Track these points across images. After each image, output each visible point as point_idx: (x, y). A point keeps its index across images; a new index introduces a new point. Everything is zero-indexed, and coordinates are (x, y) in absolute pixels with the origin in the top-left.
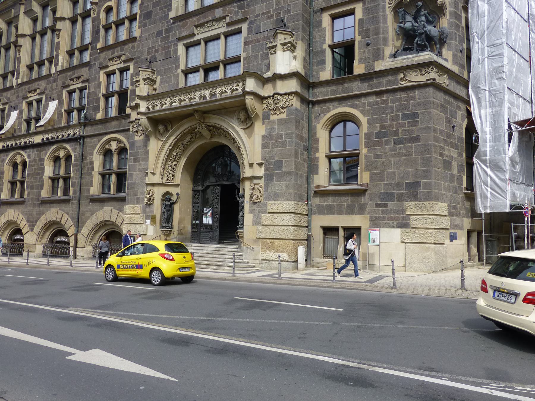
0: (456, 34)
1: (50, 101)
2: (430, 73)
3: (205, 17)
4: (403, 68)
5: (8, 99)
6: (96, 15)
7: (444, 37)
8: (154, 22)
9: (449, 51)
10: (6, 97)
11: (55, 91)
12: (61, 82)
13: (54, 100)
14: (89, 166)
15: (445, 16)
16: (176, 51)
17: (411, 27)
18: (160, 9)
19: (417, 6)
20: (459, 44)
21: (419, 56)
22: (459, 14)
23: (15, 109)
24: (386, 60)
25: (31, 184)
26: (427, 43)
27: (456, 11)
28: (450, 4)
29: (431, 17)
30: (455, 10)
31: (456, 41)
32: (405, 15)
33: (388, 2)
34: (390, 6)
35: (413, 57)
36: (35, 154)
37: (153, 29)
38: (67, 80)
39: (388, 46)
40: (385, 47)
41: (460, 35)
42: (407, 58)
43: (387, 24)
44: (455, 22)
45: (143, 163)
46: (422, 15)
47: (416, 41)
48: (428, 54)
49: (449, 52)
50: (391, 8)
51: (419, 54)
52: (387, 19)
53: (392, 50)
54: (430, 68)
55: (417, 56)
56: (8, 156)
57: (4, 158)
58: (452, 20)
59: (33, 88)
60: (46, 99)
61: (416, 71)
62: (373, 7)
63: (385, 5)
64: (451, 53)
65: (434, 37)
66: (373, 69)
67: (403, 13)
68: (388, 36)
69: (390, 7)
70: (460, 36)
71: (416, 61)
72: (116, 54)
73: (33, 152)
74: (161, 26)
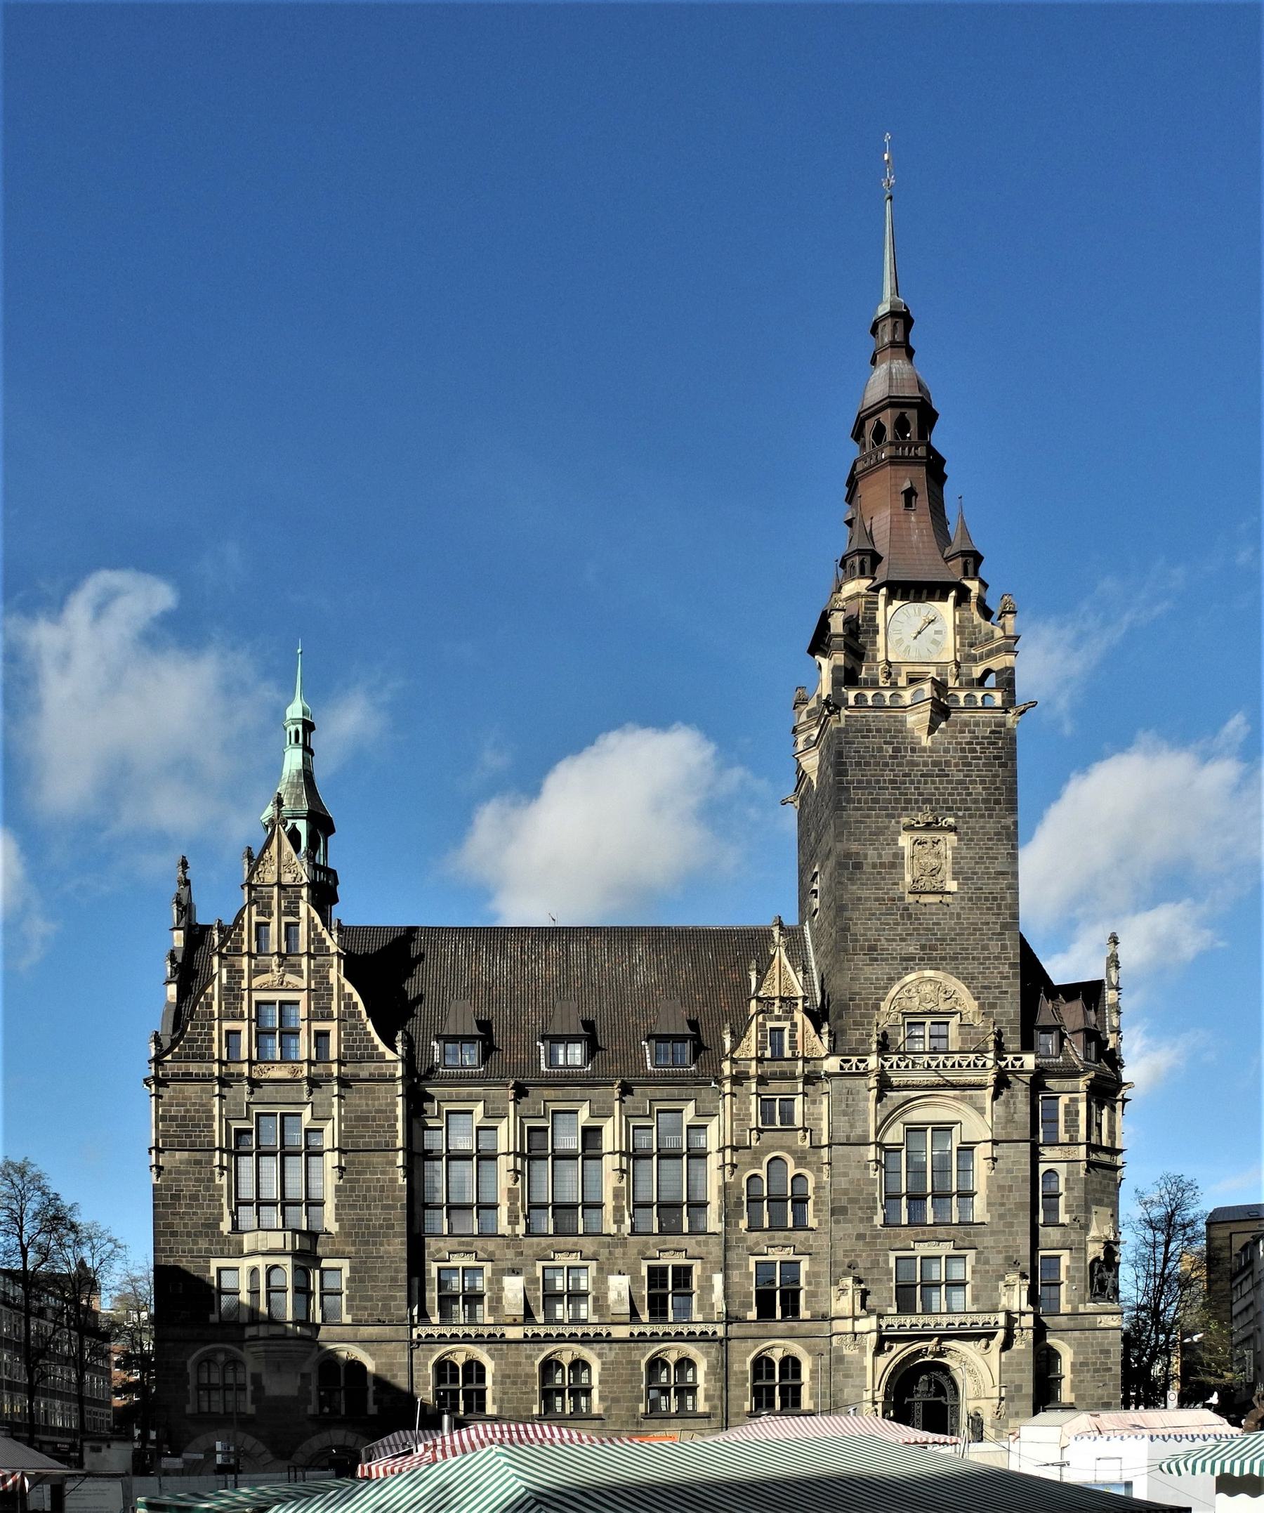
1: (612, 1274)
3: (924, 1233)
5: (492, 1253)
6: (732, 1180)
8: (851, 1222)
10: (483, 1250)
11: (620, 1262)
12: (635, 1251)
13: (620, 1273)
14: (740, 1376)
16: (887, 1262)
18: (860, 1208)
23: (515, 1272)
25: (611, 1395)
36: (617, 1354)
37: (848, 1229)
38: (648, 1249)
45: (858, 1379)
56: (542, 1350)
57: (534, 1353)
59: (562, 1248)
60: (600, 1270)
72: (776, 1242)
73: (610, 1349)
74: (861, 1228)
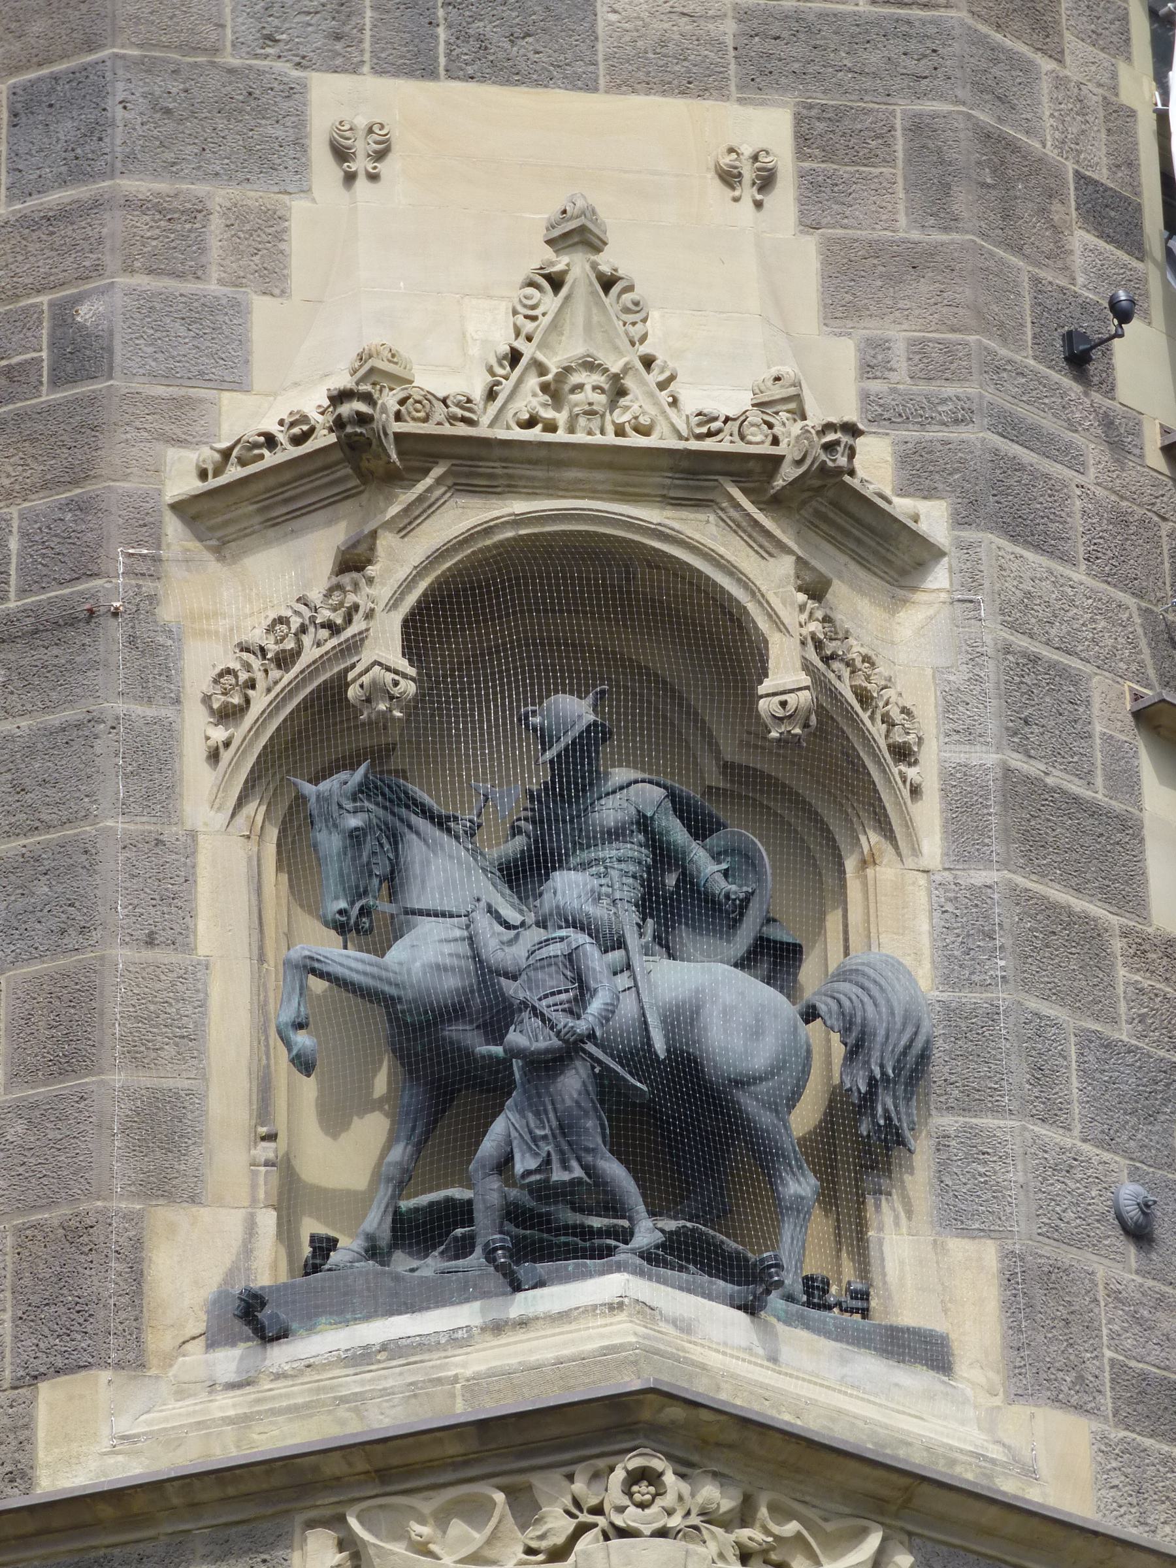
0: (1040, 1027)
2: (624, 1533)
4: (334, 1467)
7: (872, 1083)
9: (966, 1233)
15: (888, 833)
17: (451, 983)
19: (545, 739)
20: (1108, 1143)
21: (523, 1323)
22: (1098, 794)
24: (168, 1360)
26: (614, 1170)
27: (1033, 768)
28: (950, 704)
29: (716, 857)
30: (1017, 761)
31: (1052, 1114)
32: (395, 839)
33: (207, 699)
34: (219, 734)
35: (457, 1340)
39: (193, 1200)
40: (163, 1215)
41: (1124, 1034)
42: (393, 1349)
43: (182, 940)
44: (1018, 896)
46: (615, 834)
47: (490, 1145)
48: (615, 1307)
49: (958, 1247)
50: (235, 766)
51: (524, 1303)
52: (189, 880)
53: (247, 1250)
54: (619, 1475)
55: (497, 1328)
58: (981, 877)
61: (476, 1512)
62: (30, 751)
63: (169, 732)
64: (989, 1253)
65: (741, 1082)
66: (21, 1475)
67: (354, 822)
68: (204, 1077)
69: (226, 756)
70: (1109, 1045)
71: (474, 1386)
